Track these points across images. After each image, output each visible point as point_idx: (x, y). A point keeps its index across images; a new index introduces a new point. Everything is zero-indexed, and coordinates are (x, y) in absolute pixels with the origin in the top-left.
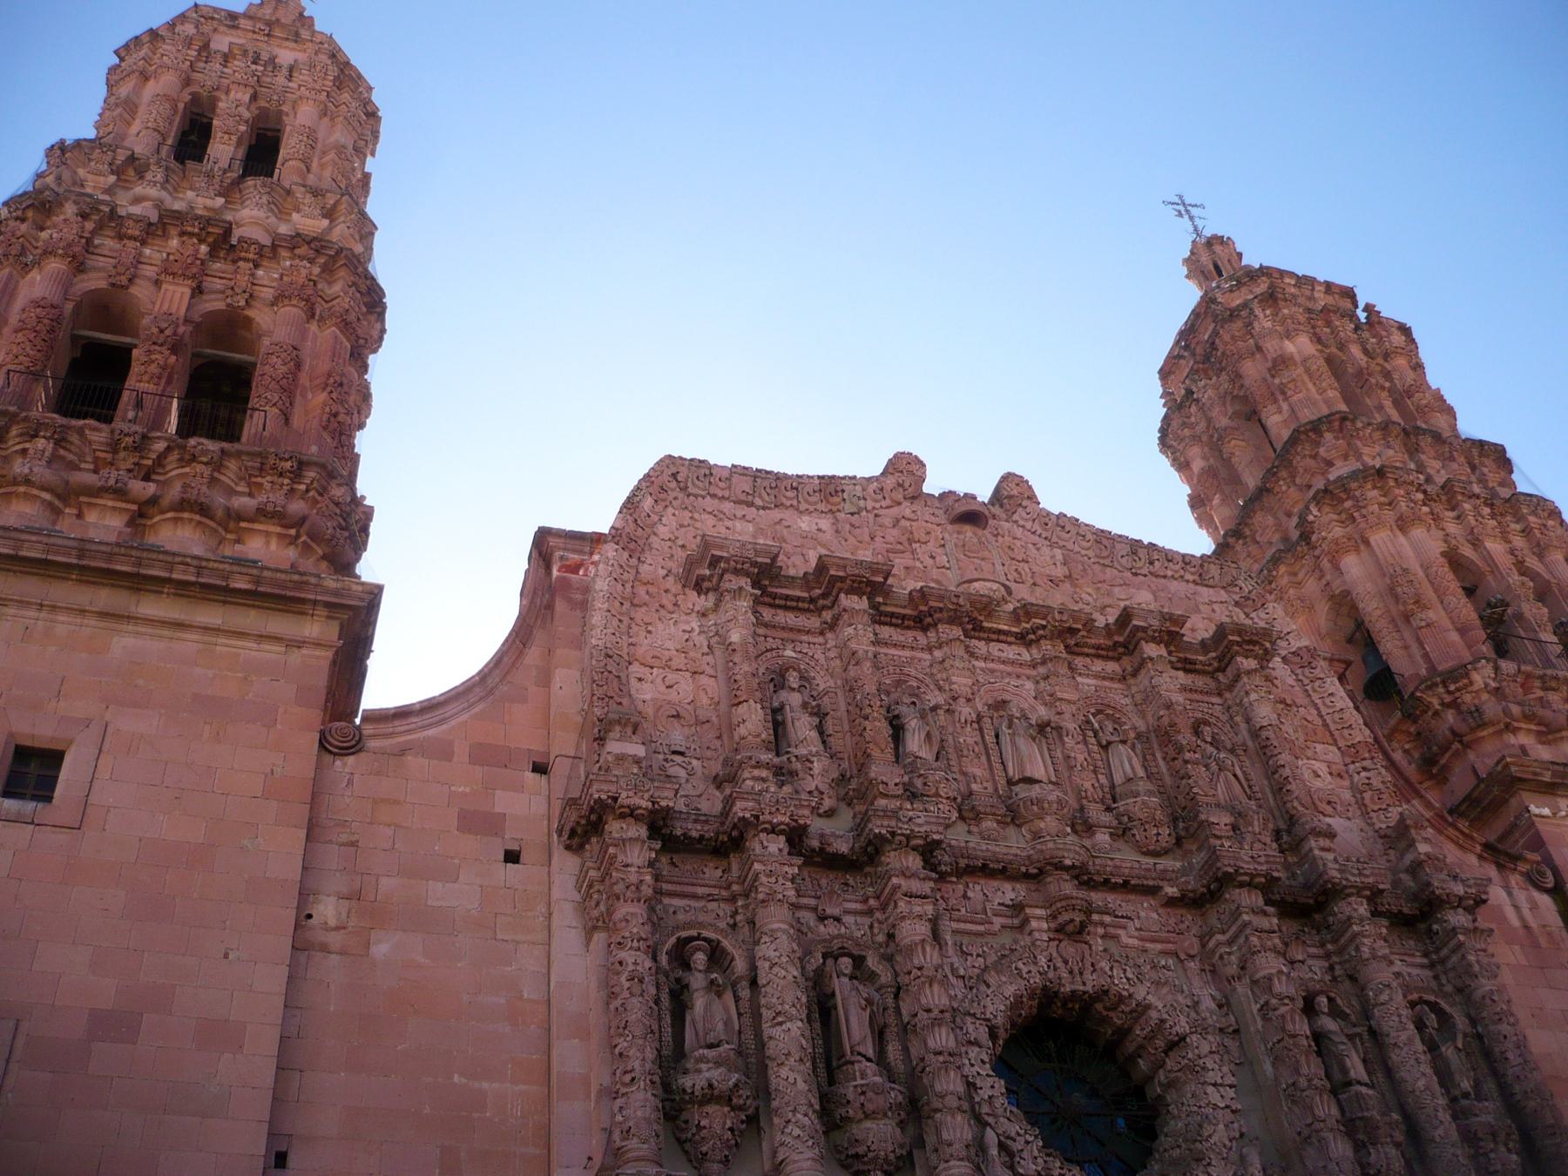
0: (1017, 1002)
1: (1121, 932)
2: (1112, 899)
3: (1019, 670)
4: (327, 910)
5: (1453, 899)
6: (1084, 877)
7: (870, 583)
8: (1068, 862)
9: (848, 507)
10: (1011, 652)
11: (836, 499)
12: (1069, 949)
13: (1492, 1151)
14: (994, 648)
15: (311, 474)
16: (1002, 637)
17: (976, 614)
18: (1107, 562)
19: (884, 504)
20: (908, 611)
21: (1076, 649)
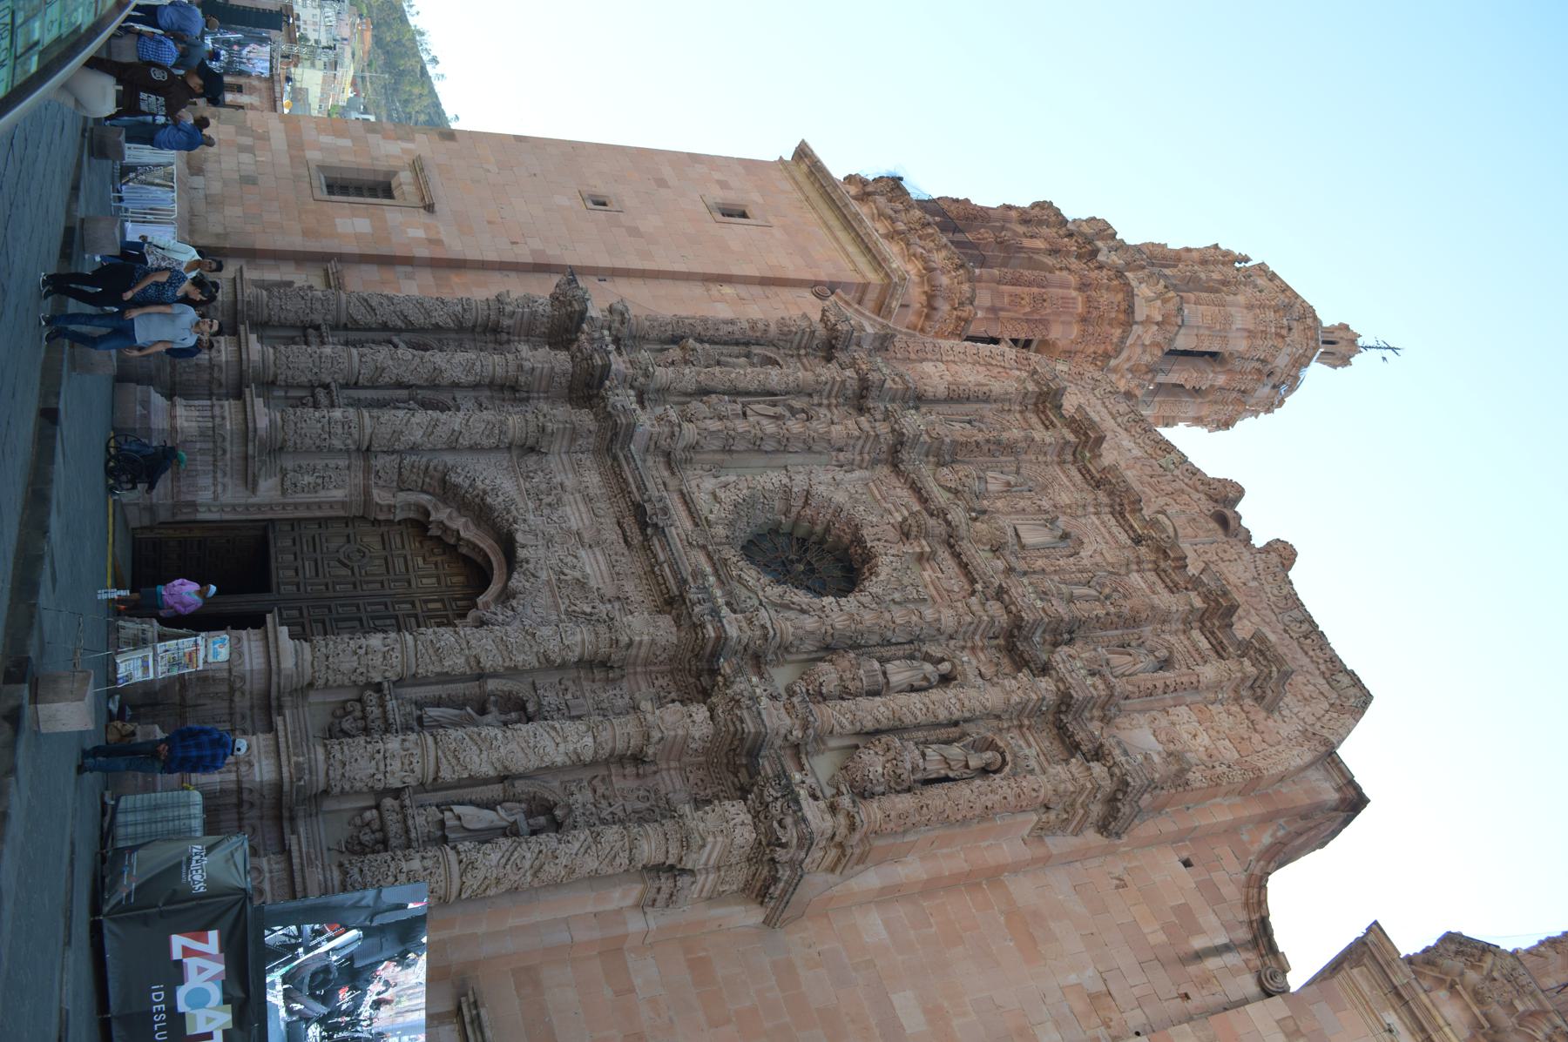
0: (839, 510)
1: (930, 572)
2: (950, 564)
3: (1111, 541)
4: (727, 290)
5: (1109, 758)
6: (951, 542)
7: (1086, 434)
8: (949, 517)
9: (1162, 462)
10: (1123, 538)
11: (1160, 452)
12: (892, 535)
13: (876, 753)
14: (1116, 530)
15: (961, 271)
16: (1131, 532)
17: (1126, 501)
18: (1277, 610)
19: (1186, 480)
20: (1098, 476)
21: (1163, 574)
